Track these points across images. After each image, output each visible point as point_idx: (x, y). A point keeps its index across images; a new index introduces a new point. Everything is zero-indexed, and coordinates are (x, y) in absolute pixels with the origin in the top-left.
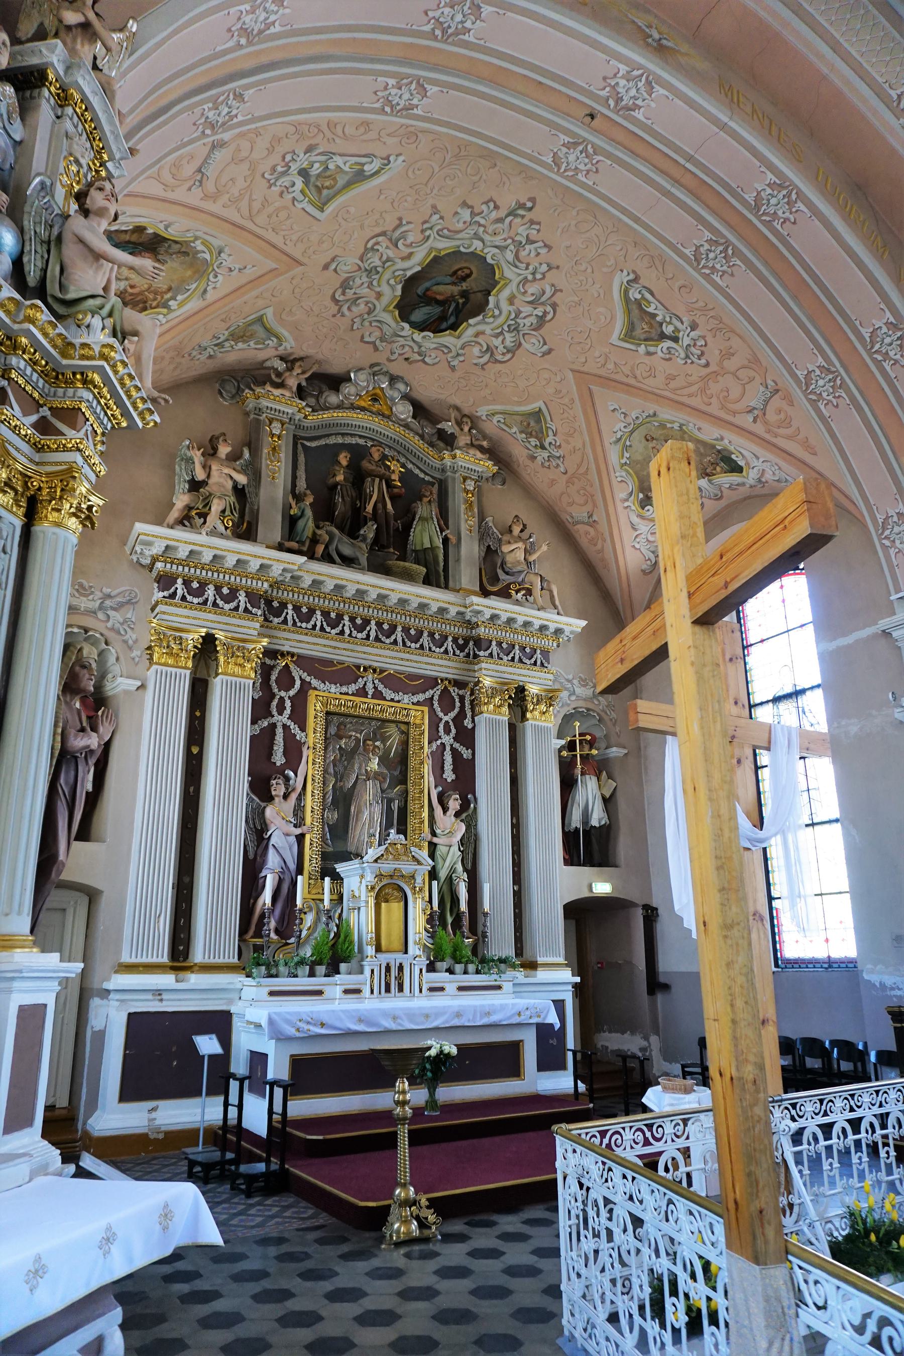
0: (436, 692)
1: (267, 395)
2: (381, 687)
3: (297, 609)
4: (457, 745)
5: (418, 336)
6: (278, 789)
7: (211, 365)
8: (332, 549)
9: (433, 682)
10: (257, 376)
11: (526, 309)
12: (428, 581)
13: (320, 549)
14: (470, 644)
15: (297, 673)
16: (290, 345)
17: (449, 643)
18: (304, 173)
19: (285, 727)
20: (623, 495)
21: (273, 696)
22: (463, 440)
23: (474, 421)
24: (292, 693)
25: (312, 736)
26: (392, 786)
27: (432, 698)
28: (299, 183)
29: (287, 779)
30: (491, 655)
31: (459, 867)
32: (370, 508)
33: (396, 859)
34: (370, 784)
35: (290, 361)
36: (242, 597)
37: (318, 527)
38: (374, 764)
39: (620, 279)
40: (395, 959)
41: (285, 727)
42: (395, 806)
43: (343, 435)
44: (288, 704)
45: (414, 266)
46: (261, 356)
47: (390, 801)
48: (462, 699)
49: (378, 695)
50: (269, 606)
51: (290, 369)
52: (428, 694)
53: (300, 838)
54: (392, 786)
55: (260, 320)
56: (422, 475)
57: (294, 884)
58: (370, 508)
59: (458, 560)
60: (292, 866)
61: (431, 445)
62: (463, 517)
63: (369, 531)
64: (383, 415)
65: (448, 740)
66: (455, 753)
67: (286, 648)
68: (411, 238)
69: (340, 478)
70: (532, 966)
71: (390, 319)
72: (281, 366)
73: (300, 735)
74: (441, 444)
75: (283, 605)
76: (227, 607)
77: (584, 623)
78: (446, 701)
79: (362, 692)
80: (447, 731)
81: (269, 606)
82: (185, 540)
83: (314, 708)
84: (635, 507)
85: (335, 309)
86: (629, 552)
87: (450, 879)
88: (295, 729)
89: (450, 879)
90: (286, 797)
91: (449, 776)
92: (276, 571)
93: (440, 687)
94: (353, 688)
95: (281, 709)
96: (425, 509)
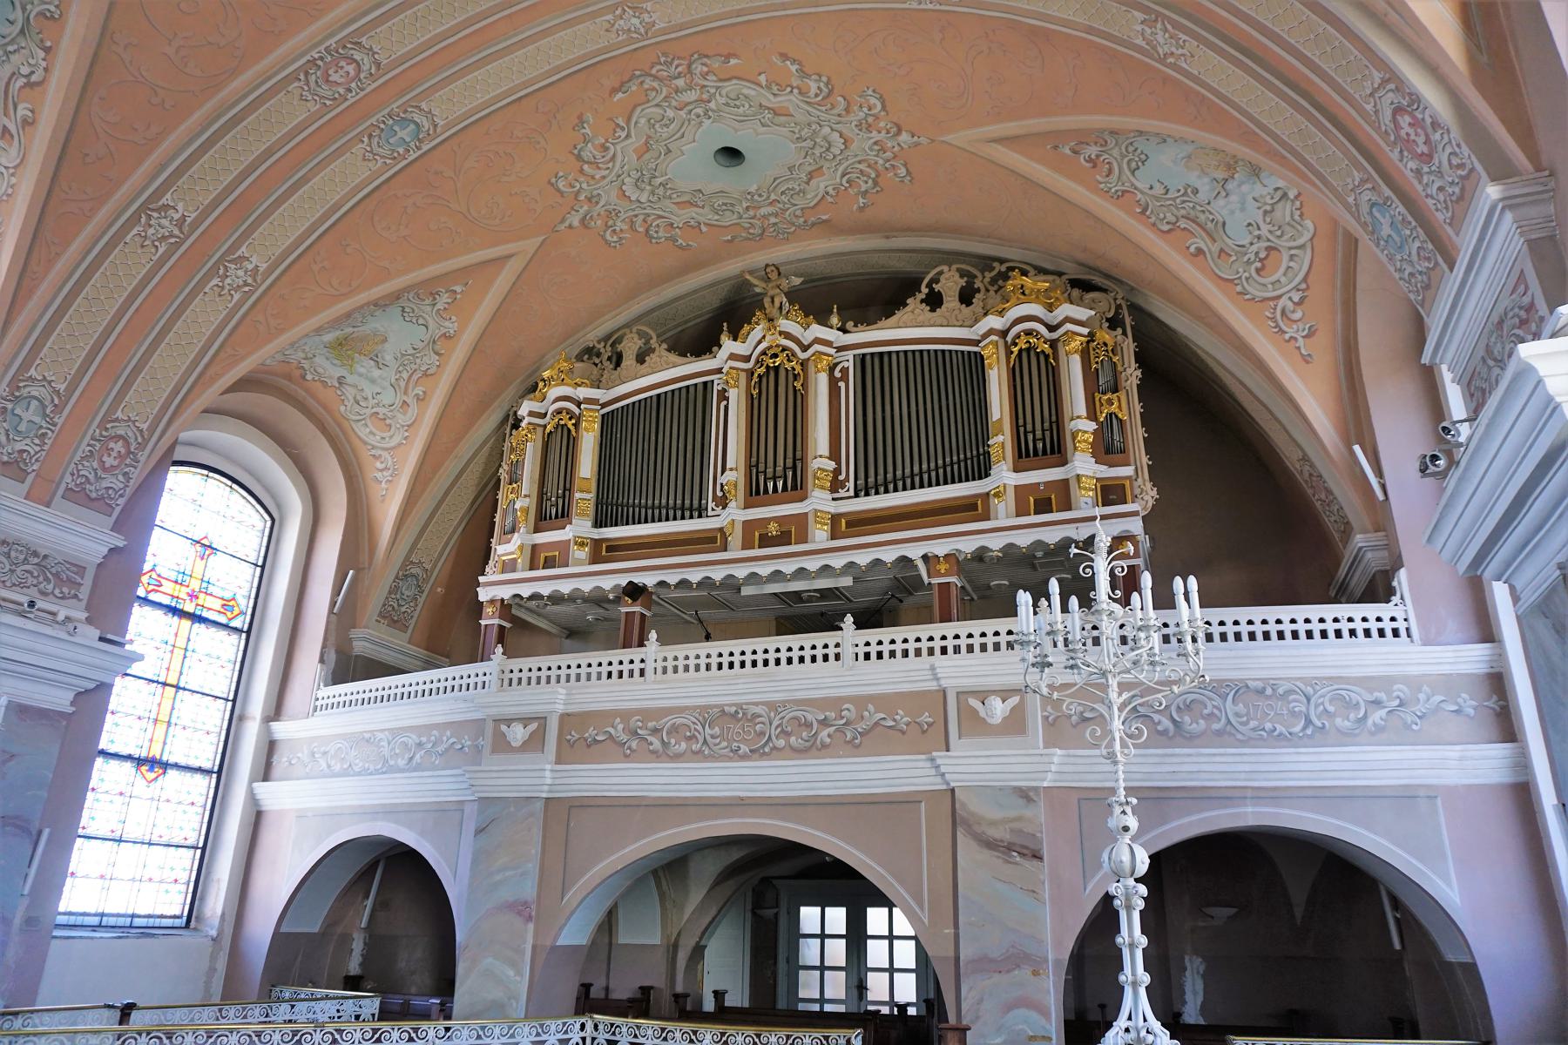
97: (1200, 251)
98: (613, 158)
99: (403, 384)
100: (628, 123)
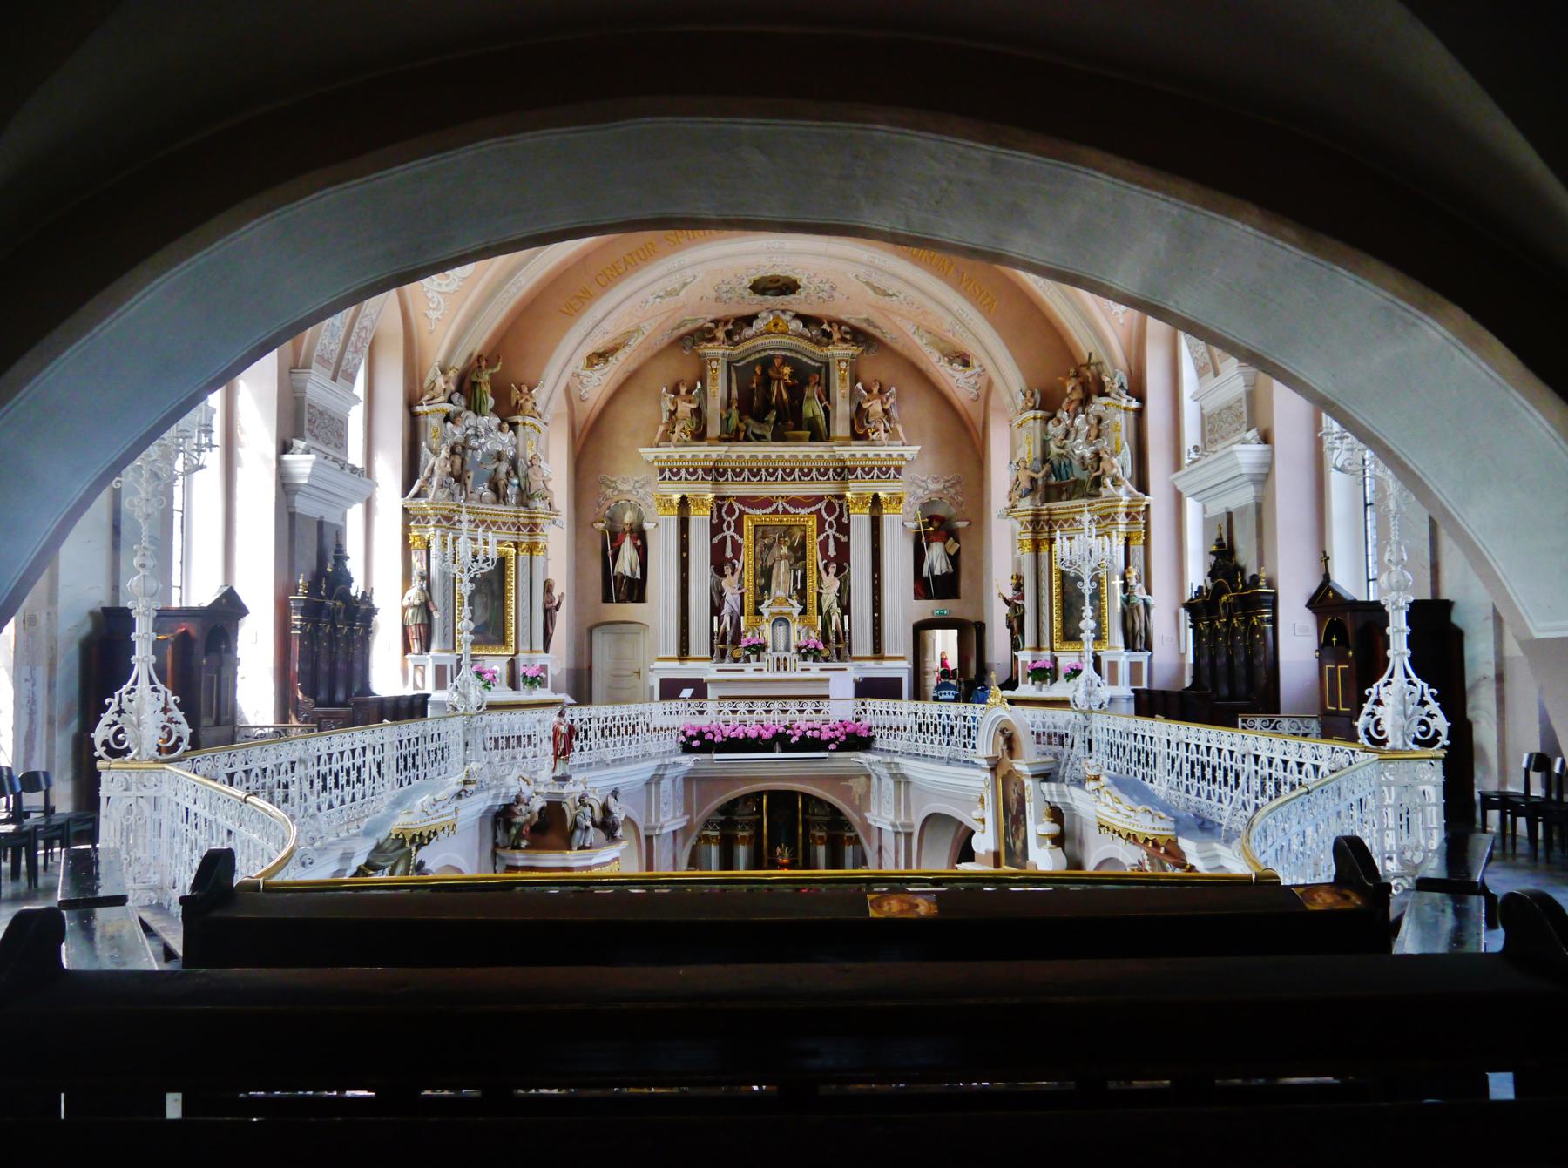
0: (823, 505)
3: (733, 470)
6: (728, 571)
9: (820, 498)
10: (703, 335)
13: (742, 435)
14: (844, 472)
15: (736, 506)
16: (711, 317)
17: (831, 472)
22: (836, 336)
23: (840, 323)
25: (747, 541)
26: (797, 561)
31: (835, 605)
35: (716, 322)
36: (700, 472)
38: (785, 550)
40: (782, 655)
48: (841, 506)
49: (786, 512)
50: (716, 472)
53: (742, 595)
54: (797, 561)
60: (737, 610)
61: (818, 343)
63: (772, 417)
65: (830, 532)
66: (836, 540)
70: (883, 658)
71: (758, 297)
72: (712, 325)
73: (740, 540)
75: (725, 470)
77: (918, 448)
78: (830, 509)
79: (776, 512)
80: (831, 526)
82: (664, 452)
83: (748, 525)
87: (828, 612)
88: (737, 537)
89: (828, 612)
91: (832, 553)
92: (714, 456)
94: (770, 510)
95: (729, 528)
96: (811, 392)
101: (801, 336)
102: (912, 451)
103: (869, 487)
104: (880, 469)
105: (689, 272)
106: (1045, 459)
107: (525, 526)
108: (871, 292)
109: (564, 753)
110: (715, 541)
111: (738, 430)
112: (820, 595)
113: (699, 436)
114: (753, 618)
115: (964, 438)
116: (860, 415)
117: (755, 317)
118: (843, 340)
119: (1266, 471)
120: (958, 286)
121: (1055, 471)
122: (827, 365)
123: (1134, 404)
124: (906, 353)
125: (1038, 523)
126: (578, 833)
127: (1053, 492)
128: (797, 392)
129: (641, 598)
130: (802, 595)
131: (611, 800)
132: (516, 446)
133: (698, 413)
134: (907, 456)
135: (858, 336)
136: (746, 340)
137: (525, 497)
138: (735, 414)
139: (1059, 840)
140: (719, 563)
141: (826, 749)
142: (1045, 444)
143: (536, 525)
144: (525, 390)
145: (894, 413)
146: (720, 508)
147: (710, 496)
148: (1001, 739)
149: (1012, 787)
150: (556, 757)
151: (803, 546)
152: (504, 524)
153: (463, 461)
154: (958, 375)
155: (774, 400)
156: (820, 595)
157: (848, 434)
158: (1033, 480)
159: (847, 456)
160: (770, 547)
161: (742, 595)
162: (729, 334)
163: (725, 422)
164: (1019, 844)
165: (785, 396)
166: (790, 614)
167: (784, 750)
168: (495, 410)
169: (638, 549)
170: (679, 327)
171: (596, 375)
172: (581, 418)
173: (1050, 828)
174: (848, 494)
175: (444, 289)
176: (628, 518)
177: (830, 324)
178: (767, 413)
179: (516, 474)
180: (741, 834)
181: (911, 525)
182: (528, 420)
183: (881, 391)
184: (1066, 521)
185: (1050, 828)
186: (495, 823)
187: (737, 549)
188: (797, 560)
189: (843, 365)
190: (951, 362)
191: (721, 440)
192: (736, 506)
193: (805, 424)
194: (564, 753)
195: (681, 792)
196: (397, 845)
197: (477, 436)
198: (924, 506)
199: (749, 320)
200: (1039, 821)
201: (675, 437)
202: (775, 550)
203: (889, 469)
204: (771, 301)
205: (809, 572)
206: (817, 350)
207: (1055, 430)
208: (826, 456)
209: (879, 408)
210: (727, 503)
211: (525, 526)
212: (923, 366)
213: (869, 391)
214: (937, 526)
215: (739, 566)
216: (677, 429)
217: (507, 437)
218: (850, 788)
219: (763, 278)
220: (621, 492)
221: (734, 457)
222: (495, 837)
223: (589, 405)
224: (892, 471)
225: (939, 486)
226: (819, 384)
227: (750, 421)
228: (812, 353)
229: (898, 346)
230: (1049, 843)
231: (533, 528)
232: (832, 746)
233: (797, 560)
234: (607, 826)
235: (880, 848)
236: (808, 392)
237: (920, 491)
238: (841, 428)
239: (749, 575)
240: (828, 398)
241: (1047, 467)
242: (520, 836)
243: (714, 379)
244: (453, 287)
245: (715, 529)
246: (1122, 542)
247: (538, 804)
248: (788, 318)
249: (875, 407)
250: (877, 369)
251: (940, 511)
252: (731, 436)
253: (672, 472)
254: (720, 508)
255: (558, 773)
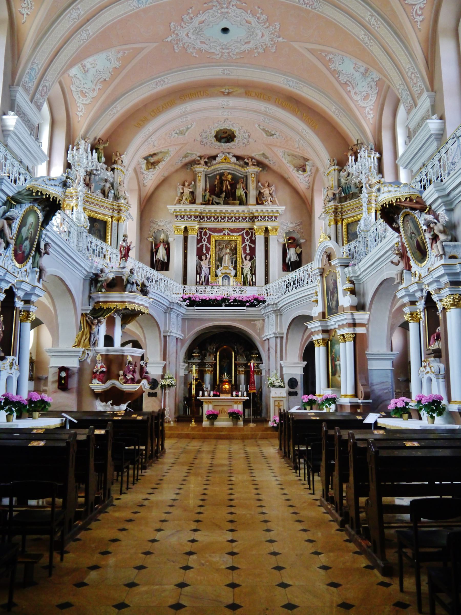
0: (244, 232)
1: (196, 167)
2: (229, 232)
3: (207, 217)
4: (250, 244)
5: (227, 144)
6: (204, 258)
7: (182, 164)
8: (214, 201)
9: (243, 229)
11: (244, 134)
12: (240, 204)
13: (211, 202)
14: (253, 218)
15: (208, 232)
16: (199, 154)
18: (176, 133)
19: (206, 244)
20: (291, 170)
21: (202, 238)
23: (252, 158)
24: (207, 237)
25: (212, 246)
27: (243, 234)
28: (176, 135)
29: (206, 256)
30: (258, 220)
31: (249, 272)
32: (224, 189)
33: (226, 270)
34: (227, 255)
35: (200, 157)
36: (193, 217)
37: (210, 197)
38: (228, 251)
39: (256, 126)
41: (206, 244)
42: (234, 260)
43: (218, 171)
44: (206, 239)
45: (214, 134)
46: (193, 158)
47: (232, 259)
48: (252, 233)
49: (228, 234)
50: (200, 217)
51: (201, 159)
52: (242, 233)
55: (187, 153)
56: (241, 176)
57: (208, 278)
58: (224, 189)
59: (250, 197)
60: (207, 274)
61: (243, 167)
62: (251, 185)
63: (223, 195)
64: (228, 163)
65: (247, 243)
66: (250, 246)
67: (205, 227)
68: (208, 131)
69: (216, 183)
71: (218, 143)
73: (209, 246)
74: (246, 166)
75: (204, 217)
76: (190, 220)
78: (247, 234)
79: (224, 234)
80: (247, 241)
81: (200, 217)
82: (178, 207)
83: (213, 240)
84: (296, 172)
85: (203, 146)
86: (300, 183)
87: (246, 276)
88: (208, 244)
90: (206, 259)
91: (248, 251)
92: (199, 210)
93: (246, 230)
94: (222, 234)
95: (204, 240)
97: (350, 91)
98: (191, 23)
99: (95, 82)
100: (203, 13)
101: (235, 164)
102: (281, 209)
103: (264, 224)
104: (268, 217)
105: (189, 117)
106: (339, 185)
107: (116, 210)
108: (265, 135)
109: (124, 257)
110: (199, 246)
111: (209, 200)
112: (242, 268)
113: (193, 202)
114: (214, 278)
115: (303, 205)
116: (260, 194)
117: (217, 156)
118: (254, 165)
119: (441, 132)
120: (301, 119)
121: (344, 190)
122: (246, 176)
123: (378, 155)
124: (279, 170)
125: (337, 213)
126: (129, 286)
127: (342, 200)
128: (234, 185)
129: (167, 269)
130: (235, 268)
131: (146, 281)
132: (114, 178)
133: (192, 193)
134: (280, 211)
135: (259, 164)
136: (213, 165)
137: (116, 198)
138: (208, 194)
139: (353, 292)
140: (200, 255)
141: (244, 306)
142: (339, 180)
143: (121, 210)
144: (118, 154)
145: (274, 195)
146: (201, 232)
147: (197, 227)
148: (325, 256)
149: (330, 278)
150: (121, 258)
151: (236, 249)
152: (107, 207)
153: (90, 179)
154: (301, 177)
155: (224, 190)
156: (242, 268)
157: (255, 203)
158: (334, 195)
159: (254, 210)
160: (222, 249)
161: (209, 268)
162: (206, 163)
163: (204, 197)
164: (334, 303)
165: (229, 187)
166: (230, 274)
167: (226, 306)
168: (105, 163)
169: (166, 249)
170: (185, 157)
171: (150, 174)
172: (144, 194)
173: (348, 286)
174: (255, 227)
175: (84, 102)
176: (162, 236)
177: (248, 159)
178: (221, 193)
179: (113, 188)
180: (207, 369)
181: (282, 241)
182: (119, 167)
183: (269, 186)
184: (349, 210)
185: (348, 286)
186: (91, 284)
187: (208, 249)
188: (233, 255)
189: (253, 175)
190: (298, 170)
191: (202, 204)
192: (208, 232)
193: (237, 198)
194: (124, 257)
195: (180, 323)
196: (28, 193)
197: (97, 170)
198: (287, 234)
199: (214, 157)
200: (343, 284)
201: (182, 202)
202: (224, 250)
203: (272, 217)
204: (225, 146)
205: (238, 259)
206: (242, 170)
207: (343, 174)
208: (246, 211)
209: (268, 192)
210: (204, 231)
211: (116, 210)
212: (286, 176)
213: (264, 186)
214: (292, 241)
215: (208, 256)
216: (184, 199)
217: (109, 173)
218: (255, 325)
219: (220, 130)
220: (159, 226)
221: (207, 211)
222: (90, 290)
223: (147, 188)
224: (273, 218)
225: (293, 225)
226: (243, 183)
227: (214, 197)
228: (240, 171)
229: (275, 168)
230: (349, 293)
231: (119, 211)
232: (248, 304)
233: (233, 255)
234: (144, 292)
235: (269, 349)
236: (238, 186)
237: (285, 227)
238: (252, 200)
239: (213, 260)
240: (247, 188)
241: (340, 188)
242: (102, 287)
243: (199, 180)
244: (88, 102)
245: (199, 241)
246: (374, 212)
247: (111, 276)
248: (230, 156)
249: (266, 192)
250: (266, 177)
251: (294, 236)
252: (206, 203)
253: (180, 217)
254: (201, 232)
255: (122, 266)
